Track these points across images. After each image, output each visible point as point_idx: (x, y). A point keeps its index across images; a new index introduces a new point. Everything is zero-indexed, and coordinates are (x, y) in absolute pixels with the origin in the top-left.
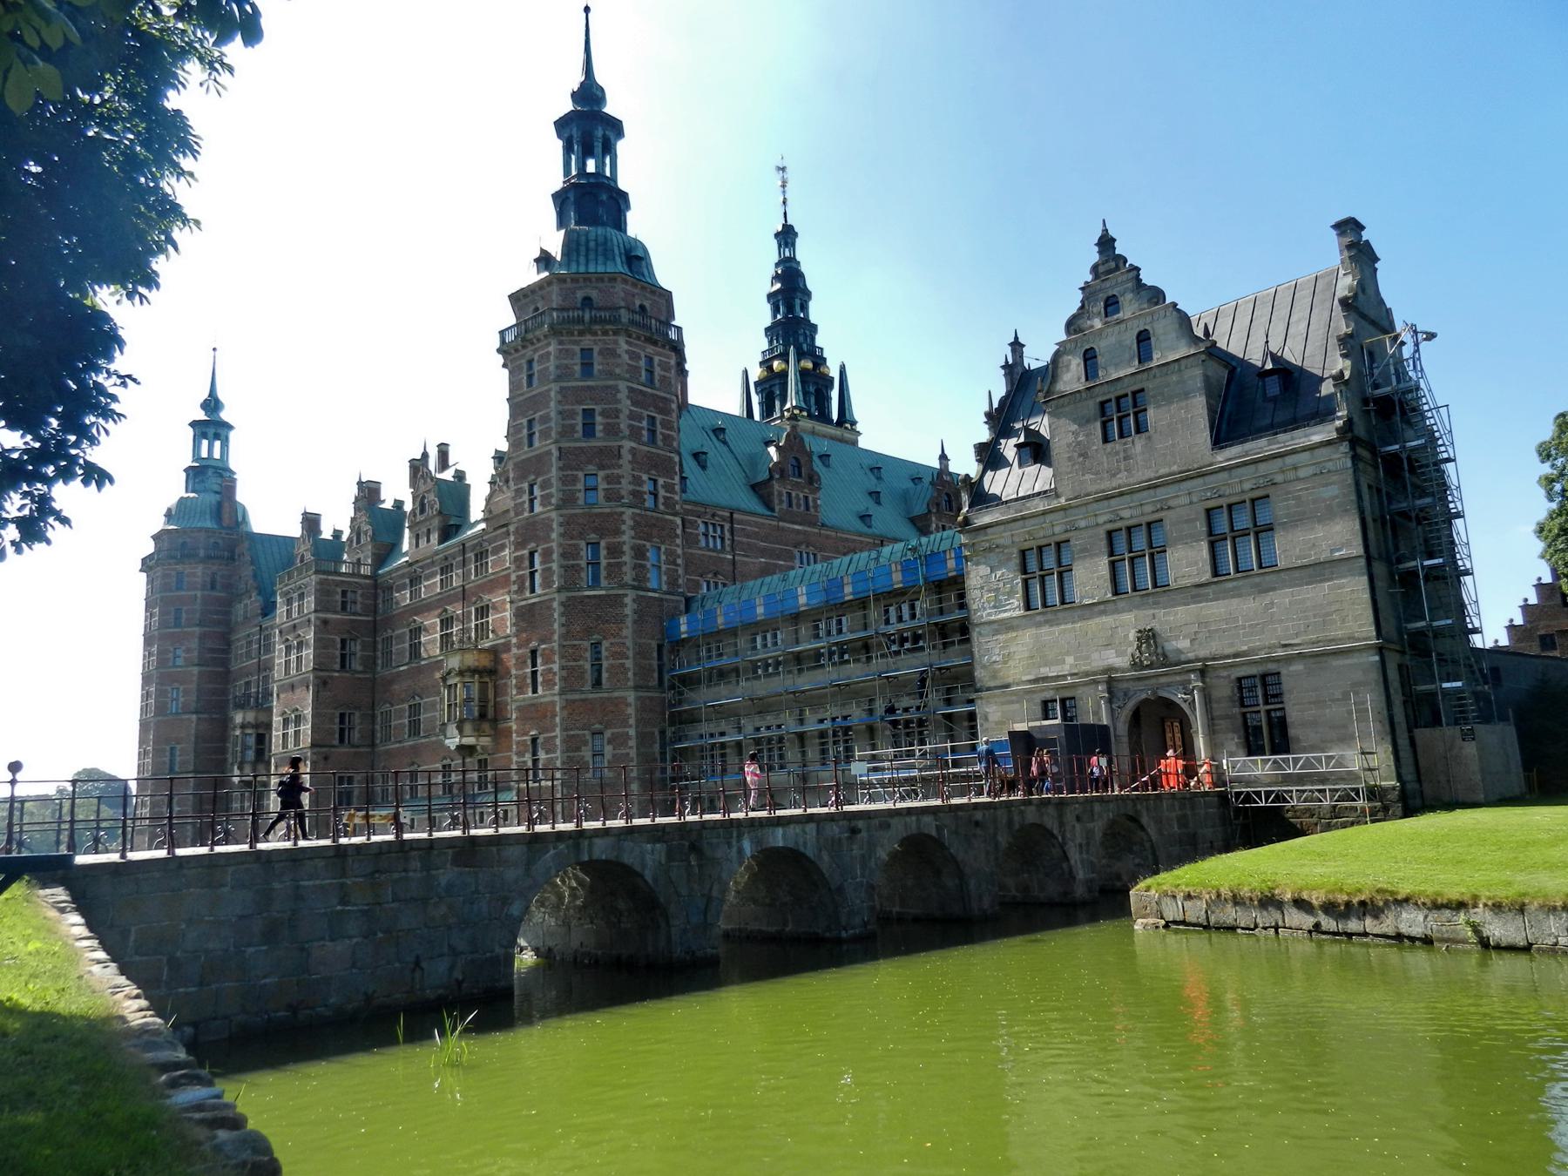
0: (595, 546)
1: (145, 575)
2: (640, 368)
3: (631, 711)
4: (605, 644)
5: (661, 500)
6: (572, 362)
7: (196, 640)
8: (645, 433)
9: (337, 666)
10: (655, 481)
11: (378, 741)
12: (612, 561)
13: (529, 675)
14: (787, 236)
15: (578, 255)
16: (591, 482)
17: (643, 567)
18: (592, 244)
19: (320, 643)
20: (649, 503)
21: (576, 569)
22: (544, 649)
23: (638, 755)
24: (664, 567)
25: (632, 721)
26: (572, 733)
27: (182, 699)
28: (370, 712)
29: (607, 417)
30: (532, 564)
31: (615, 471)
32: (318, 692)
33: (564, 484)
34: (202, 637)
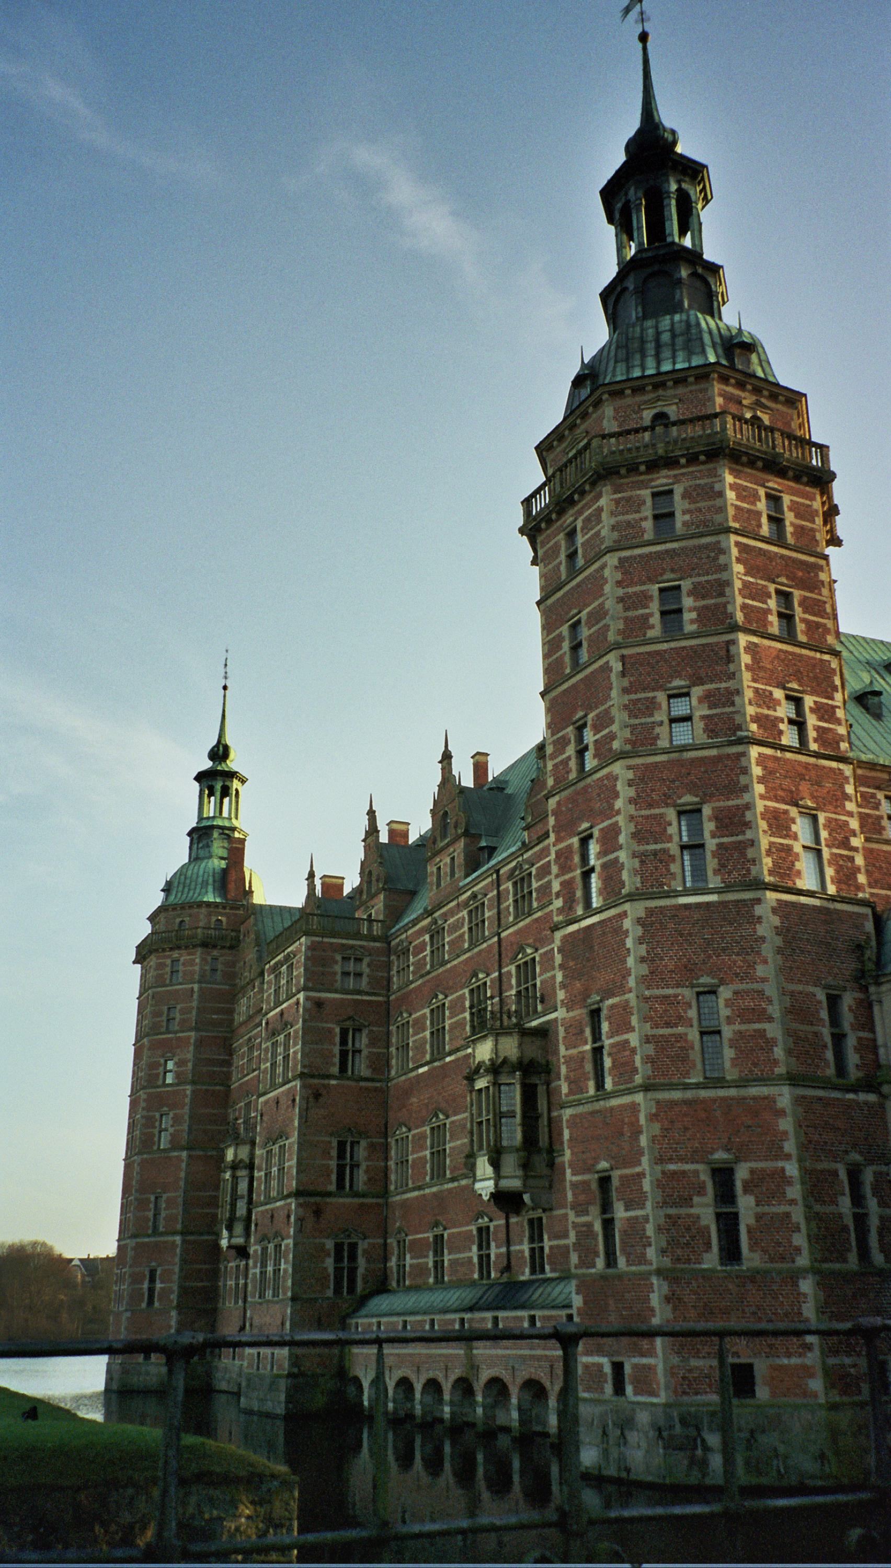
1: (139, 966)
2: (759, 514)
3: (786, 1124)
5: (812, 734)
6: (637, 516)
7: (191, 1048)
8: (773, 619)
9: (335, 1070)
10: (797, 702)
11: (392, 1188)
12: (725, 840)
13: (589, 1056)
15: (643, 356)
16: (680, 708)
17: (789, 849)
18: (666, 337)
19: (311, 1035)
20: (789, 737)
21: (664, 858)
22: (612, 1007)
23: (808, 1219)
24: (826, 853)
25: (790, 1146)
26: (672, 1167)
27: (171, 1130)
28: (382, 1140)
29: (703, 598)
30: (585, 858)
31: (723, 685)
32: (307, 1109)
33: (632, 715)
34: (200, 1043)
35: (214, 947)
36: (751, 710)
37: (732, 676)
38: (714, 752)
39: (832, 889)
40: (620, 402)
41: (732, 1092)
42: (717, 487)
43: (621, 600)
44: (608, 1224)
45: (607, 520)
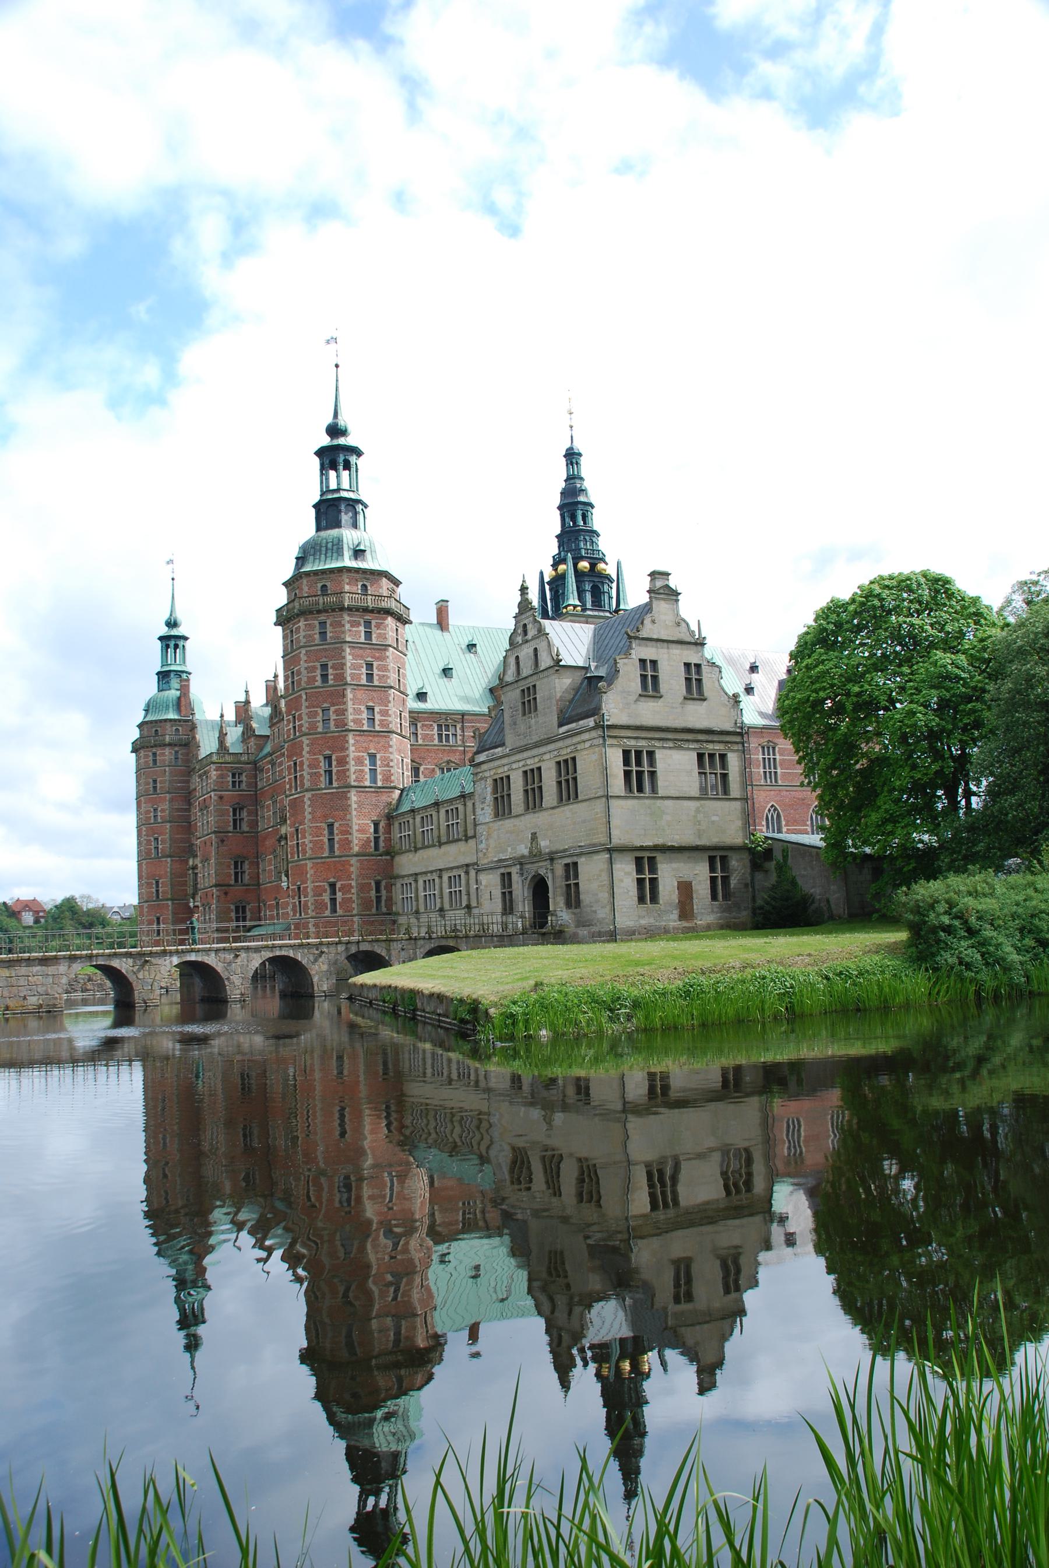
0: (329, 758)
1: (134, 754)
4: (336, 825)
9: (231, 829)
14: (572, 456)
15: (320, 554)
17: (362, 771)
18: (330, 545)
23: (357, 899)
33: (309, 718)
34: (171, 800)
35: (175, 745)
36: (351, 717)
37: (345, 703)
38: (337, 734)
39: (380, 784)
40: (309, 579)
41: (337, 859)
42: (343, 622)
43: (306, 668)
44: (300, 902)
45: (302, 634)
